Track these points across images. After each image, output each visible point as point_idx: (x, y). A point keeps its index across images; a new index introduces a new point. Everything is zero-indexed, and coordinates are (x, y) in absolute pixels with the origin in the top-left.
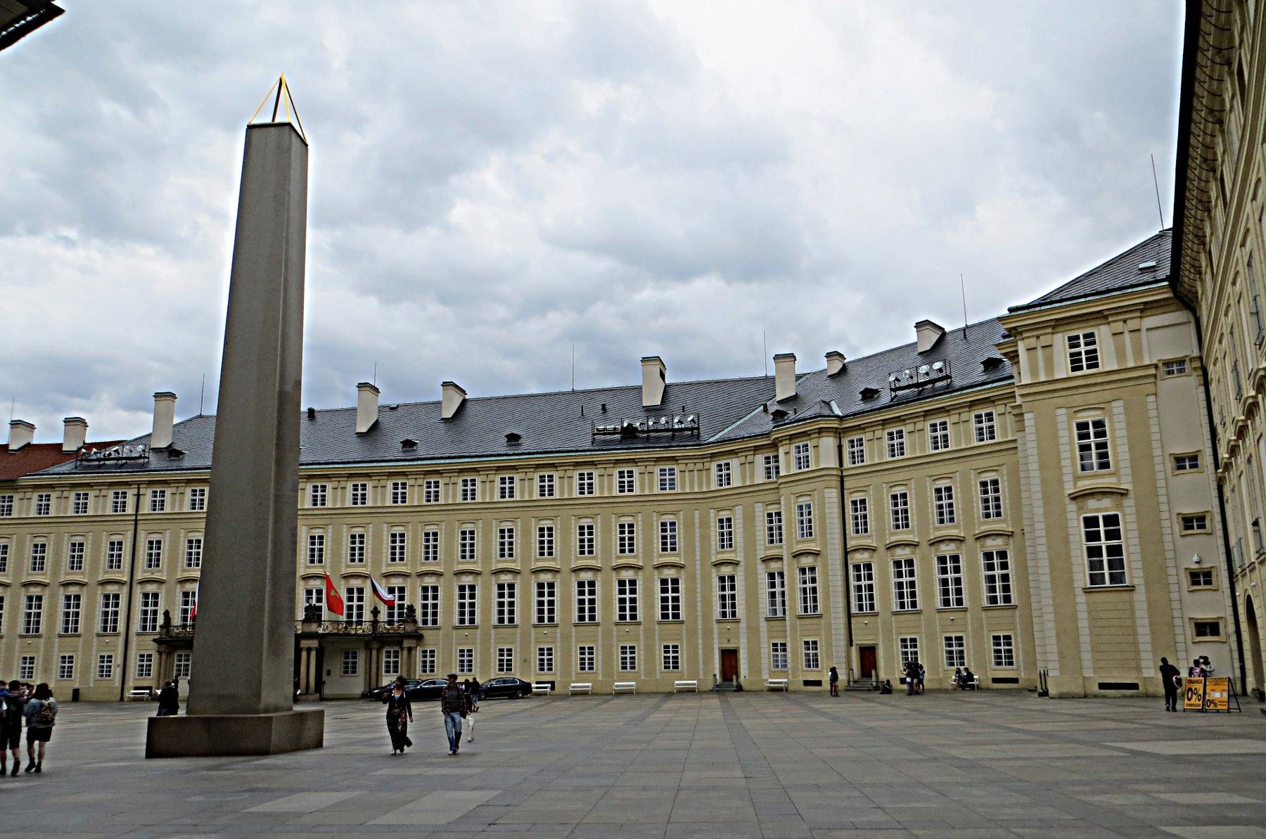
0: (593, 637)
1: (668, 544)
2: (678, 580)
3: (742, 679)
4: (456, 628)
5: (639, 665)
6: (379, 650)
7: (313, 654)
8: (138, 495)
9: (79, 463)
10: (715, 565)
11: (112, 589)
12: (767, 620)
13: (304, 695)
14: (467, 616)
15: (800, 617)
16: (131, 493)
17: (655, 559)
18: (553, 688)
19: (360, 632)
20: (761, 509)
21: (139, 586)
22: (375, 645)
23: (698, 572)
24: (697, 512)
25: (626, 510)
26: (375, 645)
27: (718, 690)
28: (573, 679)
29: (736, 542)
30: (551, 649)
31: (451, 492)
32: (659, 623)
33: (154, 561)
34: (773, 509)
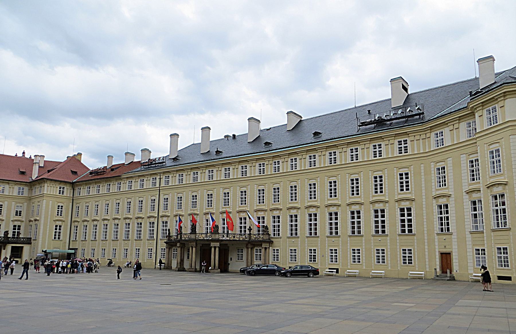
0: (361, 243)
1: (404, 186)
2: (411, 208)
3: (454, 273)
4: (289, 238)
5: (387, 260)
6: (252, 248)
7: (217, 249)
8: (160, 179)
9: (143, 167)
10: (435, 198)
11: (152, 220)
12: (471, 233)
13: (213, 269)
14: (294, 231)
15: (494, 231)
16: (158, 178)
17: (396, 196)
18: (337, 272)
19: (241, 239)
20: (465, 158)
21: (161, 219)
22: (249, 246)
23: (424, 203)
24: (422, 165)
25: (377, 168)
26: (249, 246)
27: (437, 278)
28: (349, 267)
29: (448, 182)
30: (315, 250)
31: (285, 166)
32: (399, 235)
33: (166, 207)
34: (473, 158)
